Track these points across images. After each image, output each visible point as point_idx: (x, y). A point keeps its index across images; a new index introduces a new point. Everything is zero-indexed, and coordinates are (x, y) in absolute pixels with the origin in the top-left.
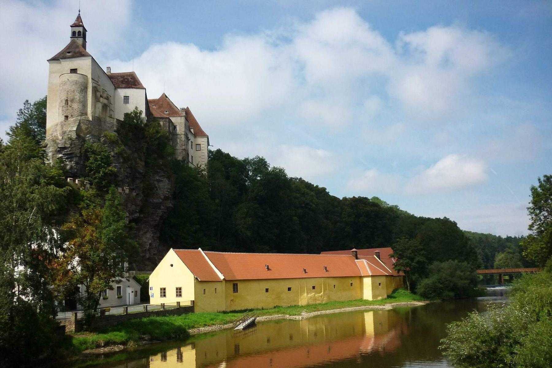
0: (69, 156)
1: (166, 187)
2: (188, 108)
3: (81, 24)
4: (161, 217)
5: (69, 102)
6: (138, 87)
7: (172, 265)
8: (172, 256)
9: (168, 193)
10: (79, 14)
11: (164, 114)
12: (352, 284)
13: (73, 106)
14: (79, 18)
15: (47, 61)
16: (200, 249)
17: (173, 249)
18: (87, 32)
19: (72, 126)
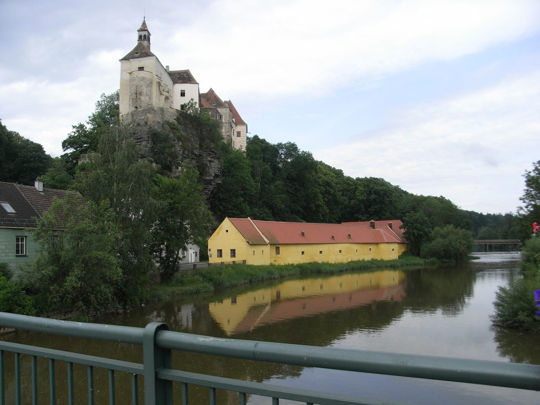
0: (139, 141)
1: (216, 167)
2: (230, 101)
3: (146, 28)
4: (212, 191)
5: (138, 95)
6: (193, 82)
7: (227, 231)
8: (227, 223)
9: (218, 171)
10: (144, 21)
11: (212, 106)
12: (370, 249)
13: (141, 99)
14: (144, 24)
15: (119, 61)
16: (249, 218)
17: (228, 217)
18: (151, 36)
19: (141, 115)
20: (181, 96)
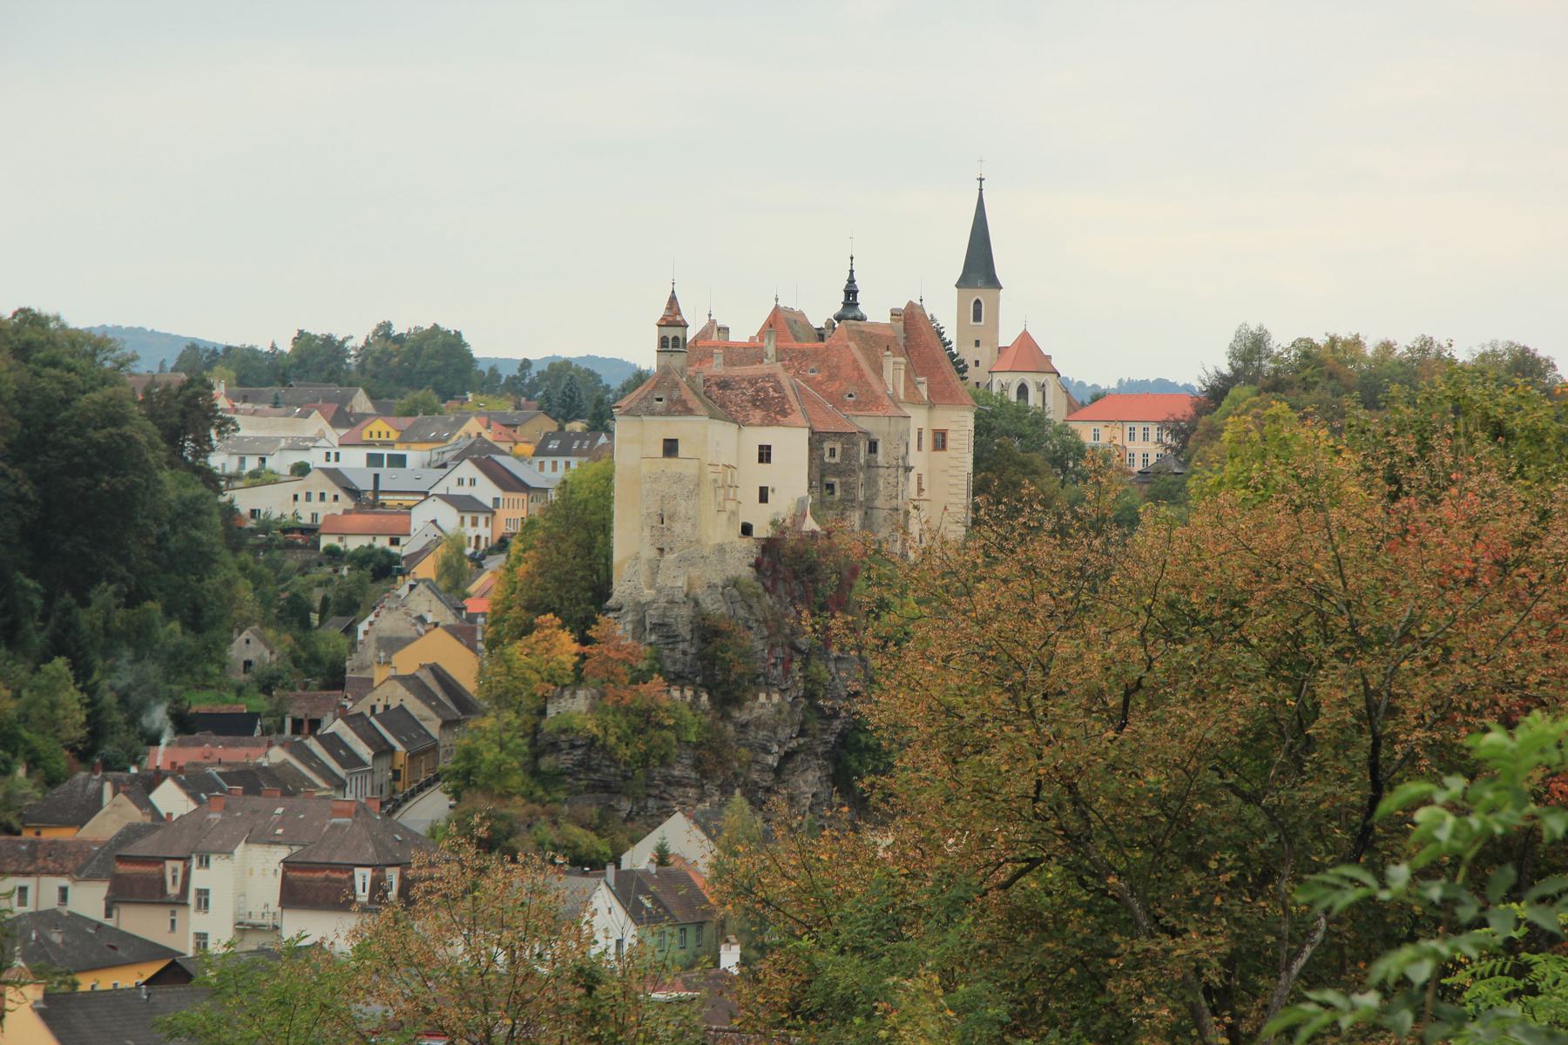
3: (678, 318)
20: (761, 461)
